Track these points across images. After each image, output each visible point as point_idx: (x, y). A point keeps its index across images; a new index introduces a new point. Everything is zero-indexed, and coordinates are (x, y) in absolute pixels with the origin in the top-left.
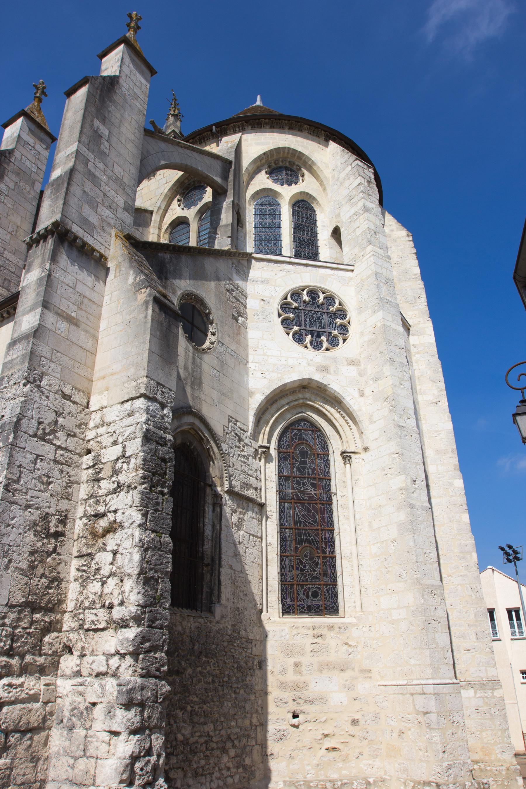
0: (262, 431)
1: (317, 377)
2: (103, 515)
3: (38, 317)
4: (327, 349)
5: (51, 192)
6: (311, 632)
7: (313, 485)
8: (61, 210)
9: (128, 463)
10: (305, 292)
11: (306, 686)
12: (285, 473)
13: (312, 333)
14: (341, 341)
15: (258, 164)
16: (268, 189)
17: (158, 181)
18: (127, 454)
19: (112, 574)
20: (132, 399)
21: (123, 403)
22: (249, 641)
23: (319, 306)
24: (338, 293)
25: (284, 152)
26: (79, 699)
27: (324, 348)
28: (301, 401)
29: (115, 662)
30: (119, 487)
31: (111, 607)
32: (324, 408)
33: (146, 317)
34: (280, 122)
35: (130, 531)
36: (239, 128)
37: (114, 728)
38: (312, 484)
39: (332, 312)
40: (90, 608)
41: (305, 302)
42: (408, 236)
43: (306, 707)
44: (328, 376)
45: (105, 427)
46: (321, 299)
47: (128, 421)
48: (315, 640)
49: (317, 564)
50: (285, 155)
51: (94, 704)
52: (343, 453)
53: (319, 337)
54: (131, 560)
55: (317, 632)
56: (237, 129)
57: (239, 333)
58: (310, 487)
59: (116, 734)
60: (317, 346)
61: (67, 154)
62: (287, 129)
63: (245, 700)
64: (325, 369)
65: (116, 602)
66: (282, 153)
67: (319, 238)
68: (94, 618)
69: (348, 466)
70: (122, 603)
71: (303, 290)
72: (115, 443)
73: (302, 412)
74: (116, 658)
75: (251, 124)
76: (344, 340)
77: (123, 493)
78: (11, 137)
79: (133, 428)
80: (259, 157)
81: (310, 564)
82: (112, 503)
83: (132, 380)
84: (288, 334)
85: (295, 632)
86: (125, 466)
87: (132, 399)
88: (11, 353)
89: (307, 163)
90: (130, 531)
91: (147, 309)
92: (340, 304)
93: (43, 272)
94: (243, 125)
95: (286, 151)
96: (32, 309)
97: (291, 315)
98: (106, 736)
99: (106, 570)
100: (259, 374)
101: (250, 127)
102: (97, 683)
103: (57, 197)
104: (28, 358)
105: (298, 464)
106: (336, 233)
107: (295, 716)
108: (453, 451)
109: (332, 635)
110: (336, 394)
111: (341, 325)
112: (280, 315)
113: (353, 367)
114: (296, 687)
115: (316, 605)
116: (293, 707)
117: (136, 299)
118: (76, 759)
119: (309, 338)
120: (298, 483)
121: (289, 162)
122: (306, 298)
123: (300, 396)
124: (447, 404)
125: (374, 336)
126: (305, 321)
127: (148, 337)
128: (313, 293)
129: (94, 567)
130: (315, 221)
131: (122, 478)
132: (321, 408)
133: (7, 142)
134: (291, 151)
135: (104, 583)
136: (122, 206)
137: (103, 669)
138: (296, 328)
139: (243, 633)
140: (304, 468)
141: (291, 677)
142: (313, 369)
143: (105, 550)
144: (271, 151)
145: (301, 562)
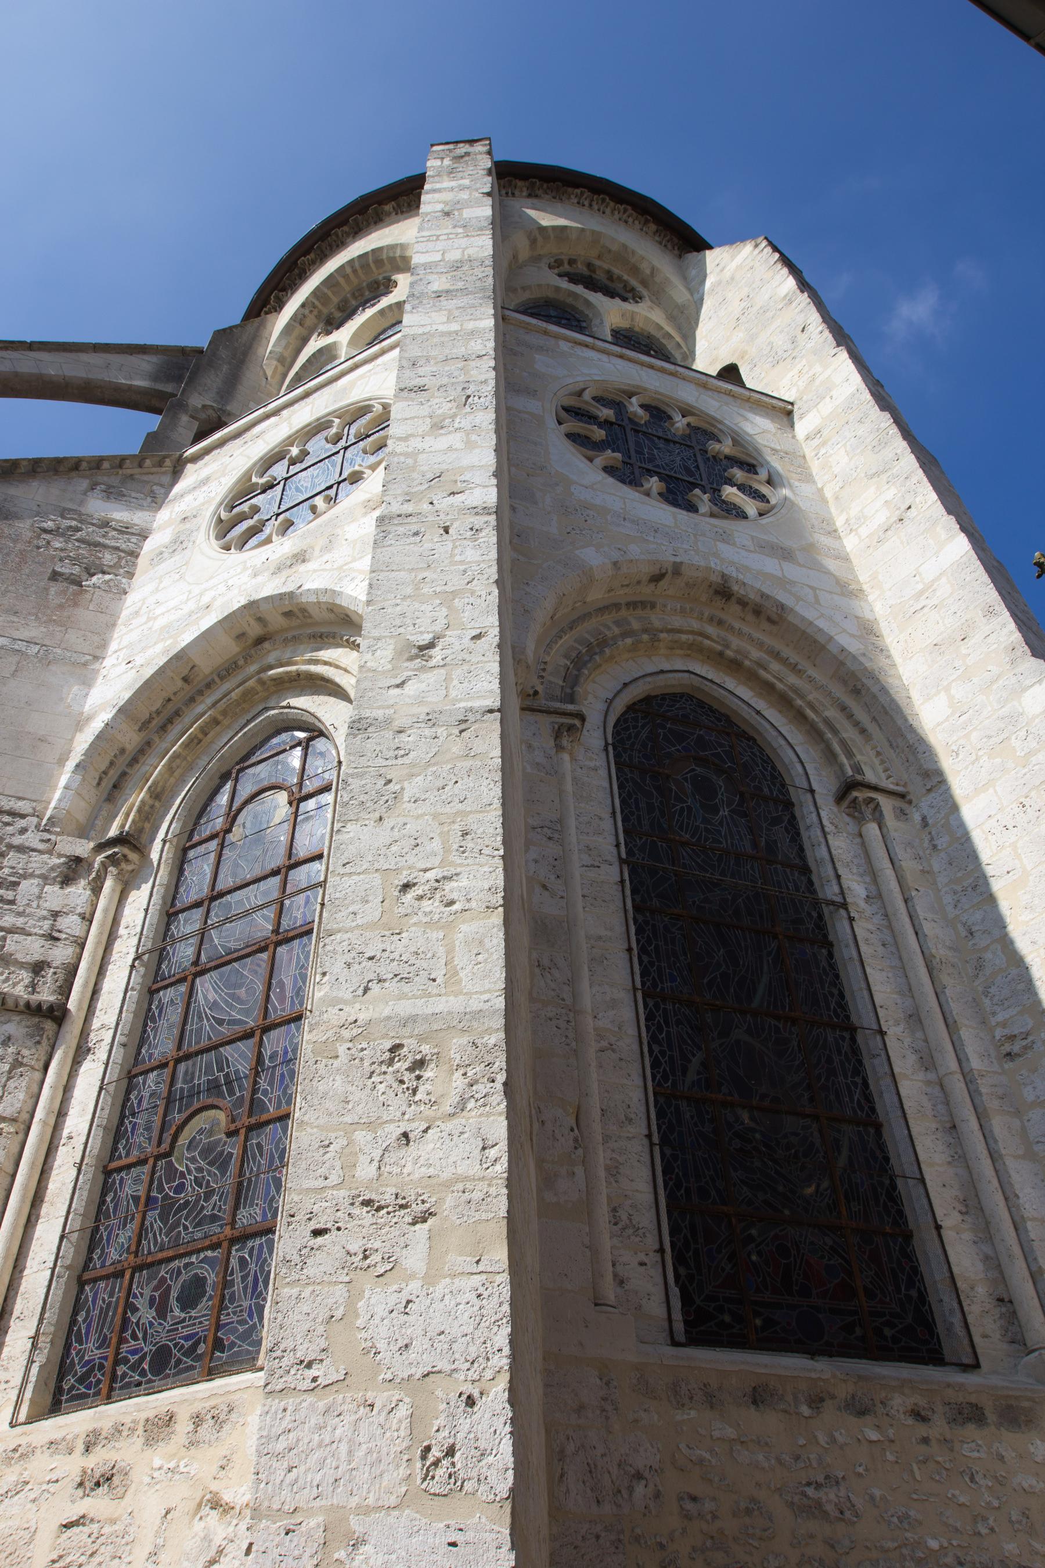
0: (124, 810)
15: (298, 330)
25: (346, 277)
32: (316, 662)
34: (334, 237)
42: (756, 246)
50: (355, 281)
55: (98, 1460)
66: (341, 281)
73: (267, 709)
81: (200, 1170)
89: (394, 258)
95: (349, 270)
108: (990, 612)
109: (157, 1462)
110: (323, 599)
115: (187, 1338)
123: (253, 668)
124: (934, 496)
132: (313, 668)
134: (357, 265)
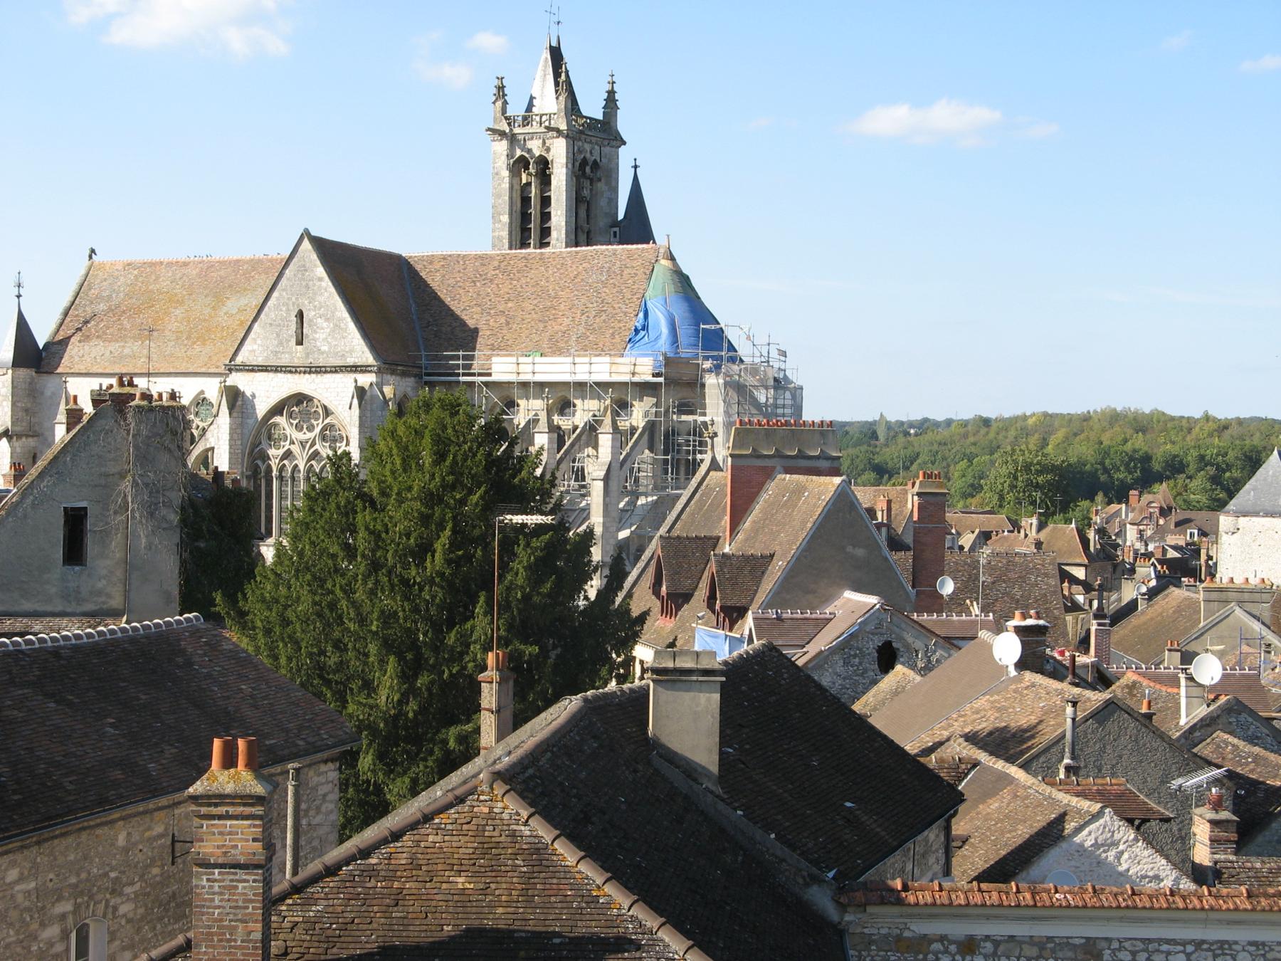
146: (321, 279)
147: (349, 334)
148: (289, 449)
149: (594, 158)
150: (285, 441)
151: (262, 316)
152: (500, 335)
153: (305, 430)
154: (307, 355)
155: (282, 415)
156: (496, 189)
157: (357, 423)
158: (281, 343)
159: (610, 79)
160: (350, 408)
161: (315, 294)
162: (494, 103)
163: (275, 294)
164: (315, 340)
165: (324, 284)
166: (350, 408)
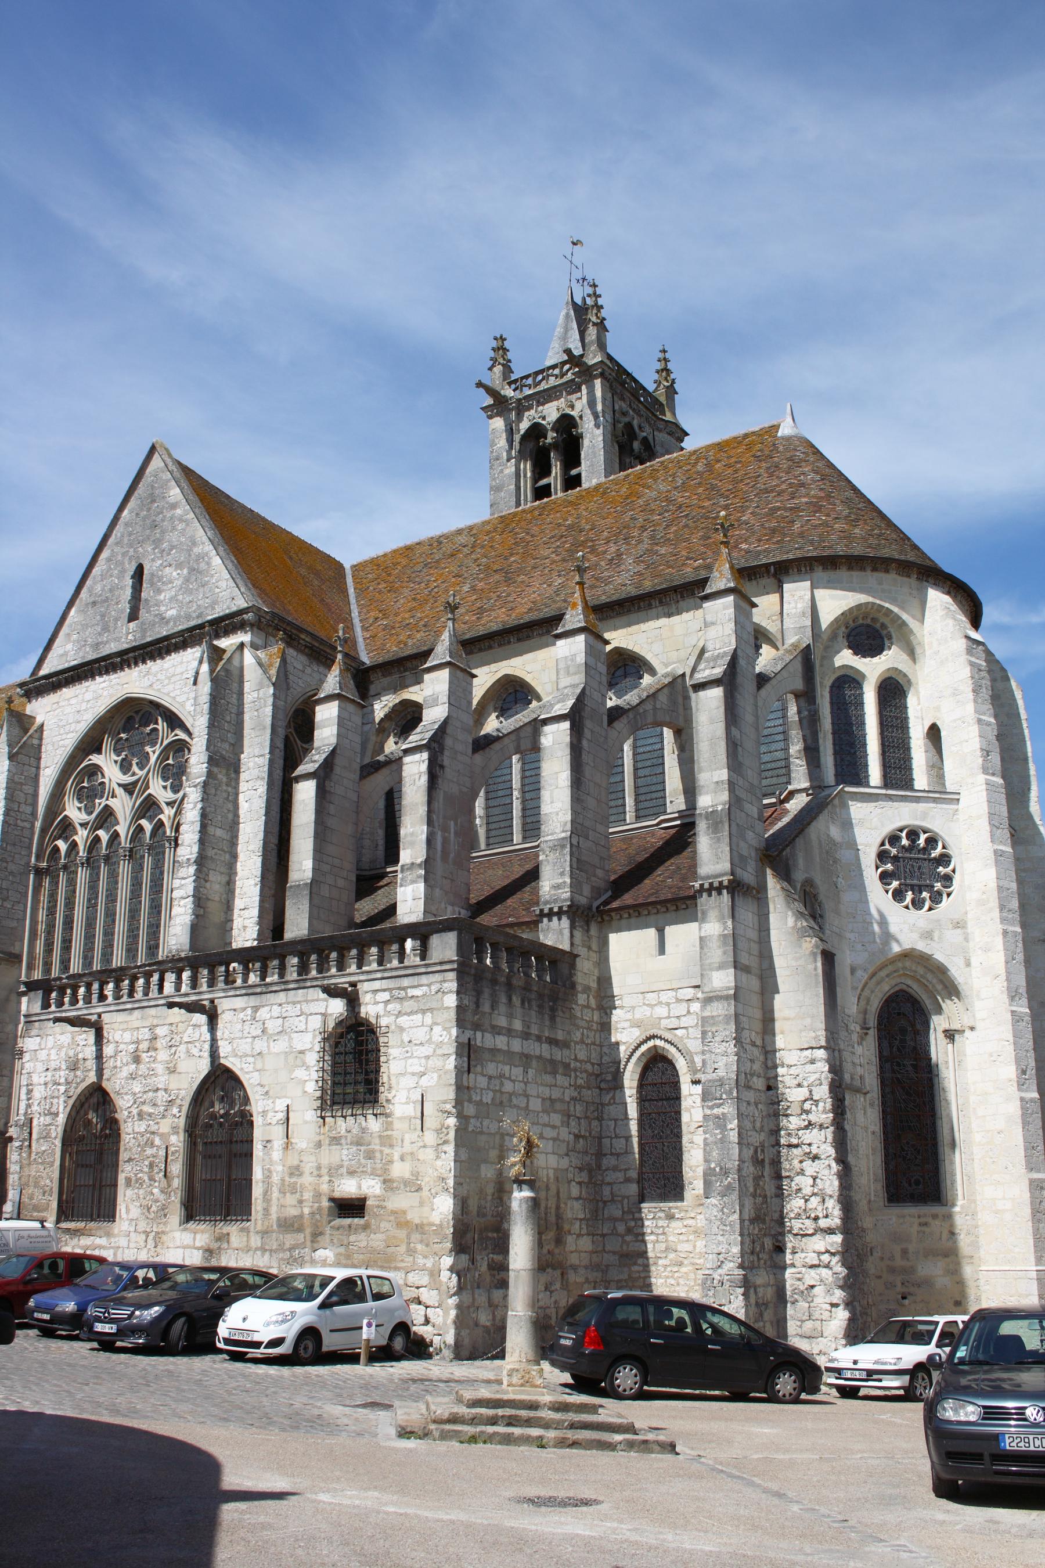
1: (921, 946)
2: (796, 1146)
3: (732, 978)
4: (930, 909)
5: (708, 828)
6: (917, 1221)
7: (915, 1067)
8: (728, 858)
9: (817, 1106)
10: (904, 834)
11: (911, 1270)
12: (885, 1054)
13: (912, 888)
14: (945, 896)
16: (847, 666)
17: (686, 622)
18: (815, 1098)
19: (814, 1194)
20: (812, 1048)
21: (802, 1050)
22: (863, 1230)
23: (919, 851)
24: (941, 833)
26: (798, 1283)
27: (927, 907)
28: (901, 972)
29: (826, 1258)
30: (810, 1125)
31: (816, 1219)
33: (816, 969)
35: (827, 1162)
36: (805, 567)
37: (835, 1301)
38: (912, 1065)
39: (935, 858)
40: (795, 1218)
41: (903, 847)
43: (912, 1289)
44: (933, 944)
45: (785, 1069)
46: (922, 841)
47: (810, 1068)
48: (920, 1228)
49: (918, 1152)
51: (812, 1287)
52: (945, 1031)
53: (921, 893)
54: (831, 1185)
55: (922, 1220)
56: (803, 569)
57: (839, 902)
58: (910, 1068)
59: (835, 1305)
60: (917, 904)
61: (715, 780)
62: (869, 569)
63: (863, 1283)
64: (928, 935)
65: (821, 1215)
67: (911, 735)
68: (802, 1226)
69: (950, 1046)
70: (827, 1216)
71: (901, 830)
72: (799, 1085)
74: (827, 1255)
75: (823, 564)
76: (949, 895)
77: (815, 1131)
78: (572, 660)
79: (817, 1076)
80: (836, 619)
82: (805, 1137)
83: (810, 1030)
84: (887, 892)
85: (901, 1220)
86: (814, 1107)
87: (812, 1048)
88: (709, 1008)
90: (827, 1162)
91: (815, 961)
92: (944, 847)
93: (725, 929)
94: (811, 565)
96: (721, 967)
97: (889, 867)
98: (828, 1307)
99: (807, 1190)
100: (859, 947)
101: (821, 568)
102: (812, 1272)
103: (719, 839)
104: (733, 1018)
105: (897, 1042)
106: (934, 733)
107: (904, 1298)
111: (945, 875)
112: (877, 868)
113: (959, 931)
114: (905, 1271)
116: (899, 1288)
117: (800, 947)
118: (803, 1321)
119: (909, 895)
120: (899, 1065)
121: (872, 619)
122: (905, 842)
123: (900, 965)
125: (984, 896)
126: (905, 872)
127: (821, 991)
128: (913, 834)
129: (794, 1187)
130: (906, 708)
131: (812, 1117)
133: (568, 667)
135: (806, 1201)
136: (756, 816)
137: (816, 1262)
138: (895, 884)
139: (860, 1223)
140: (904, 1047)
141: (899, 1262)
142: (915, 936)
143: (803, 1175)
144: (851, 610)
145: (903, 1150)
146: (174, 506)
147: (212, 576)
148: (107, 806)
149: (644, 434)
150: (102, 797)
151: (84, 594)
152: (494, 596)
153: (135, 768)
154: (144, 631)
155: (99, 751)
156: (494, 479)
157: (206, 707)
158: (106, 629)
159: (661, 355)
160: (195, 683)
161: (163, 532)
162: (490, 369)
163: (105, 554)
164: (158, 604)
165: (179, 511)
166: (195, 683)
